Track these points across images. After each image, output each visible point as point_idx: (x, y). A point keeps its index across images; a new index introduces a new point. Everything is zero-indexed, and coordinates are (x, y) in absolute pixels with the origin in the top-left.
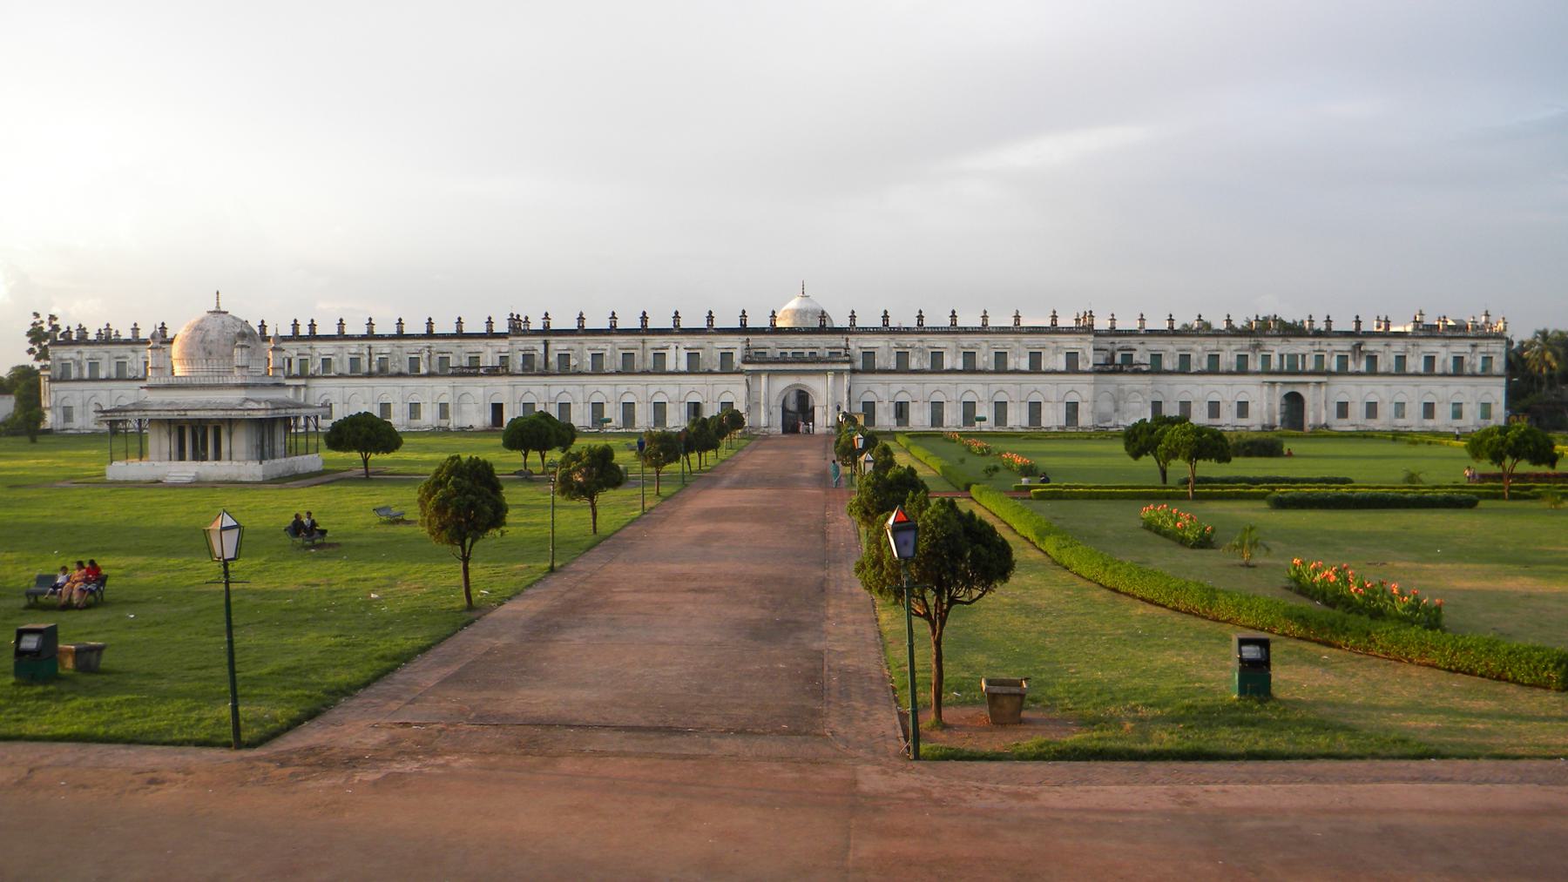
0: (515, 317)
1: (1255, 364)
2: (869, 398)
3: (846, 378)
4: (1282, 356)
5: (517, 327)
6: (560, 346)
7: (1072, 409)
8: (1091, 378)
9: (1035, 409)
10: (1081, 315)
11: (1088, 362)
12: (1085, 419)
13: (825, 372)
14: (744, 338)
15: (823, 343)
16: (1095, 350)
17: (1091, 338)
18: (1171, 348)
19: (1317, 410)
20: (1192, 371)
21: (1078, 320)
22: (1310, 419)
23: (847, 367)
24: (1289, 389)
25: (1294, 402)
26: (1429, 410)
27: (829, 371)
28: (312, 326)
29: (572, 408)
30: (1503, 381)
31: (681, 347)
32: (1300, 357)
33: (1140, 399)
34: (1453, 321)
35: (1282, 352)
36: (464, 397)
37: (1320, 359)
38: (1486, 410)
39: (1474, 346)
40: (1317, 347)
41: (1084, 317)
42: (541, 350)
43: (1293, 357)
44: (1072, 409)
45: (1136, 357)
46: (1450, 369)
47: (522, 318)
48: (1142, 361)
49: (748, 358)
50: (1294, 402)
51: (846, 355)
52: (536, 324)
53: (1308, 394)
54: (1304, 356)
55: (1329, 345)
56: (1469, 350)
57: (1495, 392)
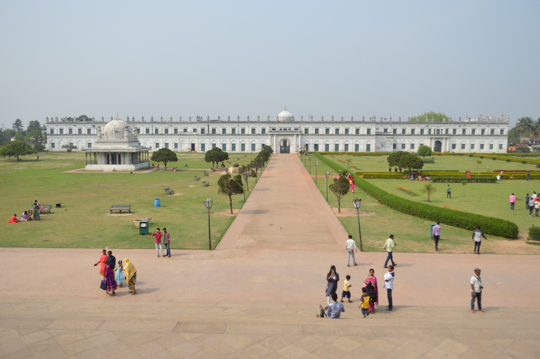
0: (198, 117)
1: (426, 132)
2: (307, 143)
3: (300, 137)
4: (435, 130)
5: (199, 121)
7: (368, 146)
8: (374, 137)
9: (357, 146)
10: (372, 118)
11: (373, 132)
12: (373, 149)
14: (269, 124)
15: (293, 127)
16: (376, 128)
17: (375, 125)
18: (399, 128)
19: (446, 147)
20: (406, 134)
21: (371, 119)
22: (443, 150)
23: (300, 133)
24: (437, 140)
25: (438, 144)
26: (482, 146)
27: (294, 135)
28: (133, 118)
29: (205, 146)
30: (507, 137)
31: (250, 127)
32: (441, 130)
33: (390, 143)
34: (492, 117)
35: (435, 129)
36: (183, 142)
38: (501, 146)
40: (446, 127)
41: (373, 118)
42: (207, 127)
43: (438, 130)
44: (368, 146)
45: (389, 131)
46: (490, 133)
47: (200, 117)
48: (390, 131)
49: (270, 131)
50: (438, 144)
51: (300, 130)
52: (205, 119)
53: (443, 142)
54: (442, 130)
55: (450, 126)
57: (505, 142)
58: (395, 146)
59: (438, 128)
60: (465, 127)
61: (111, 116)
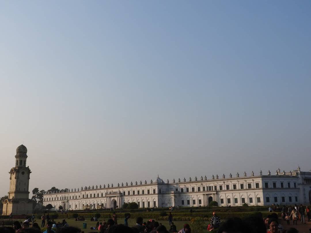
1: (202, 190)
6: (87, 193)
13: (115, 197)
37: (216, 187)
38: (259, 200)
39: (253, 180)
40: (215, 184)
43: (210, 187)
45: (179, 190)
53: (212, 196)
54: (212, 186)
56: (252, 181)
58: (183, 202)
59: (209, 186)
60: (228, 183)
61: (141, 180)
